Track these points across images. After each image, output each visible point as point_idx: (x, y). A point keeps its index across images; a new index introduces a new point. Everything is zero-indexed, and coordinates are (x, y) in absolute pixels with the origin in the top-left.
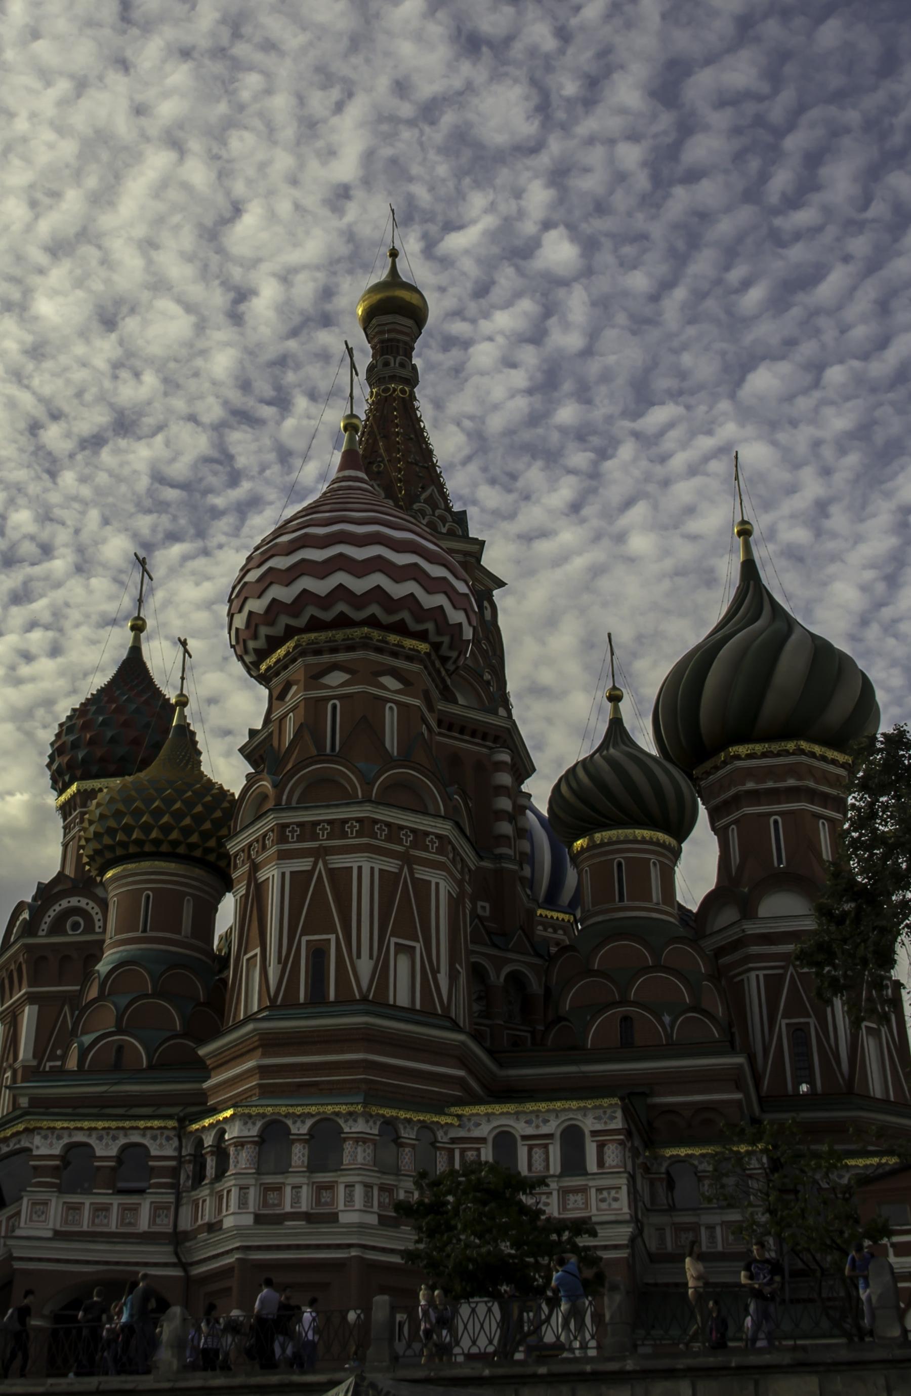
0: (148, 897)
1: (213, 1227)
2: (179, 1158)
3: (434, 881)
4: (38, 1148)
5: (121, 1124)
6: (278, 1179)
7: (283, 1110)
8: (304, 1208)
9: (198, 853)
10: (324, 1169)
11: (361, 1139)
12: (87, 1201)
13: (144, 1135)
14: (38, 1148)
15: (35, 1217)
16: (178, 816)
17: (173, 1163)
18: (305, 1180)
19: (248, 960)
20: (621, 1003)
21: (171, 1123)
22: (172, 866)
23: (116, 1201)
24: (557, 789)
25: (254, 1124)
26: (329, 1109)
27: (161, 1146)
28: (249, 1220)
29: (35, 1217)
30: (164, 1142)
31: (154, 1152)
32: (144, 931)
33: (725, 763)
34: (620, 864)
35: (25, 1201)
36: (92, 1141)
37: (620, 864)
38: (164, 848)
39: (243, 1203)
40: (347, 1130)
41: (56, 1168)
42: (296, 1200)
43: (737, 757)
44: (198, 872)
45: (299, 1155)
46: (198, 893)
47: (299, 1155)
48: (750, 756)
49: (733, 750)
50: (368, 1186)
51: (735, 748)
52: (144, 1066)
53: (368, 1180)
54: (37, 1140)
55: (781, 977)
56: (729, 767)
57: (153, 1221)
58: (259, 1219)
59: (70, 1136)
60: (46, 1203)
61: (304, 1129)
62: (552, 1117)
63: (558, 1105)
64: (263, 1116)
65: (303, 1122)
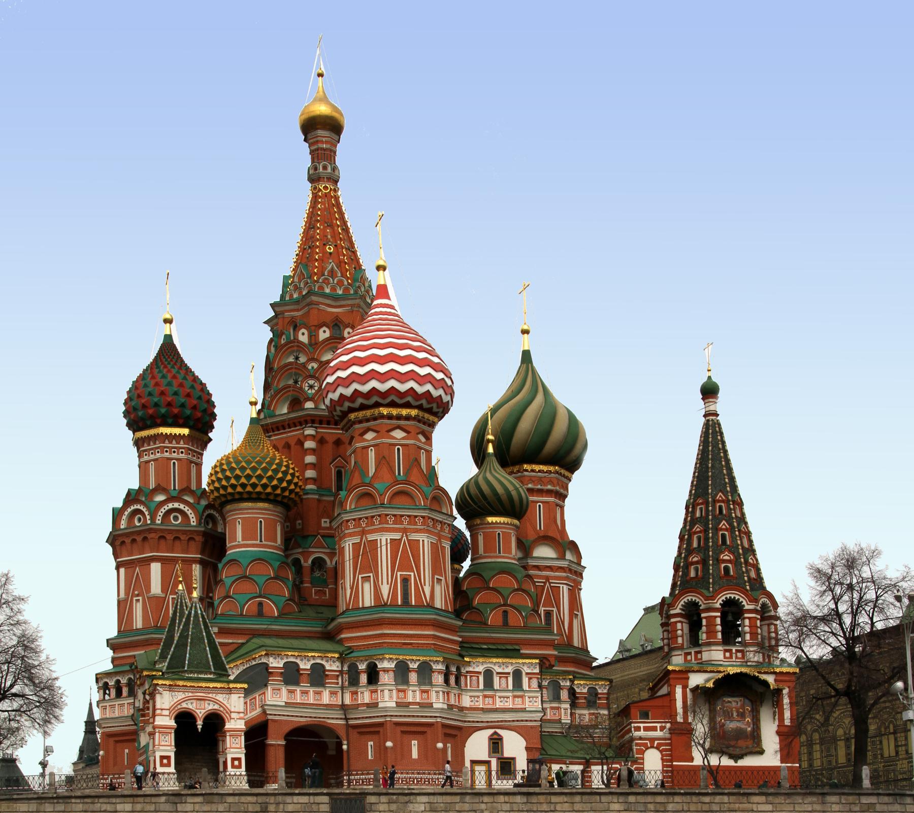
0: (261, 522)
1: (368, 705)
2: (341, 672)
3: (447, 547)
4: (272, 663)
5: (313, 654)
6: (405, 687)
7: (408, 658)
8: (418, 700)
9: (279, 499)
10: (424, 684)
11: (439, 672)
12: (298, 689)
13: (322, 660)
14: (272, 663)
15: (274, 696)
16: (271, 478)
17: (338, 673)
18: (417, 688)
19: (362, 577)
20: (504, 605)
21: (337, 655)
22: (266, 505)
23: (311, 690)
24: (462, 488)
25: (393, 662)
26: (428, 659)
27: (331, 665)
28: (394, 705)
29: (274, 696)
30: (332, 663)
31: (327, 668)
32: (261, 541)
33: (518, 471)
34: (499, 534)
35: (269, 687)
36: (298, 661)
37: (499, 534)
38: (272, 497)
39: (391, 697)
40: (434, 668)
41: (282, 673)
42: (414, 697)
43: (527, 471)
44: (279, 509)
45: (413, 677)
46: (266, 516)
47: (413, 677)
48: (533, 471)
49: (525, 466)
50: (444, 692)
51: (525, 466)
52: (276, 615)
53: (444, 690)
54: (271, 659)
55: (543, 587)
56: (520, 474)
57: (330, 700)
58: (399, 704)
59: (287, 658)
60: (279, 690)
61: (416, 666)
62: (510, 666)
63: (514, 661)
64: (397, 659)
65: (415, 663)
